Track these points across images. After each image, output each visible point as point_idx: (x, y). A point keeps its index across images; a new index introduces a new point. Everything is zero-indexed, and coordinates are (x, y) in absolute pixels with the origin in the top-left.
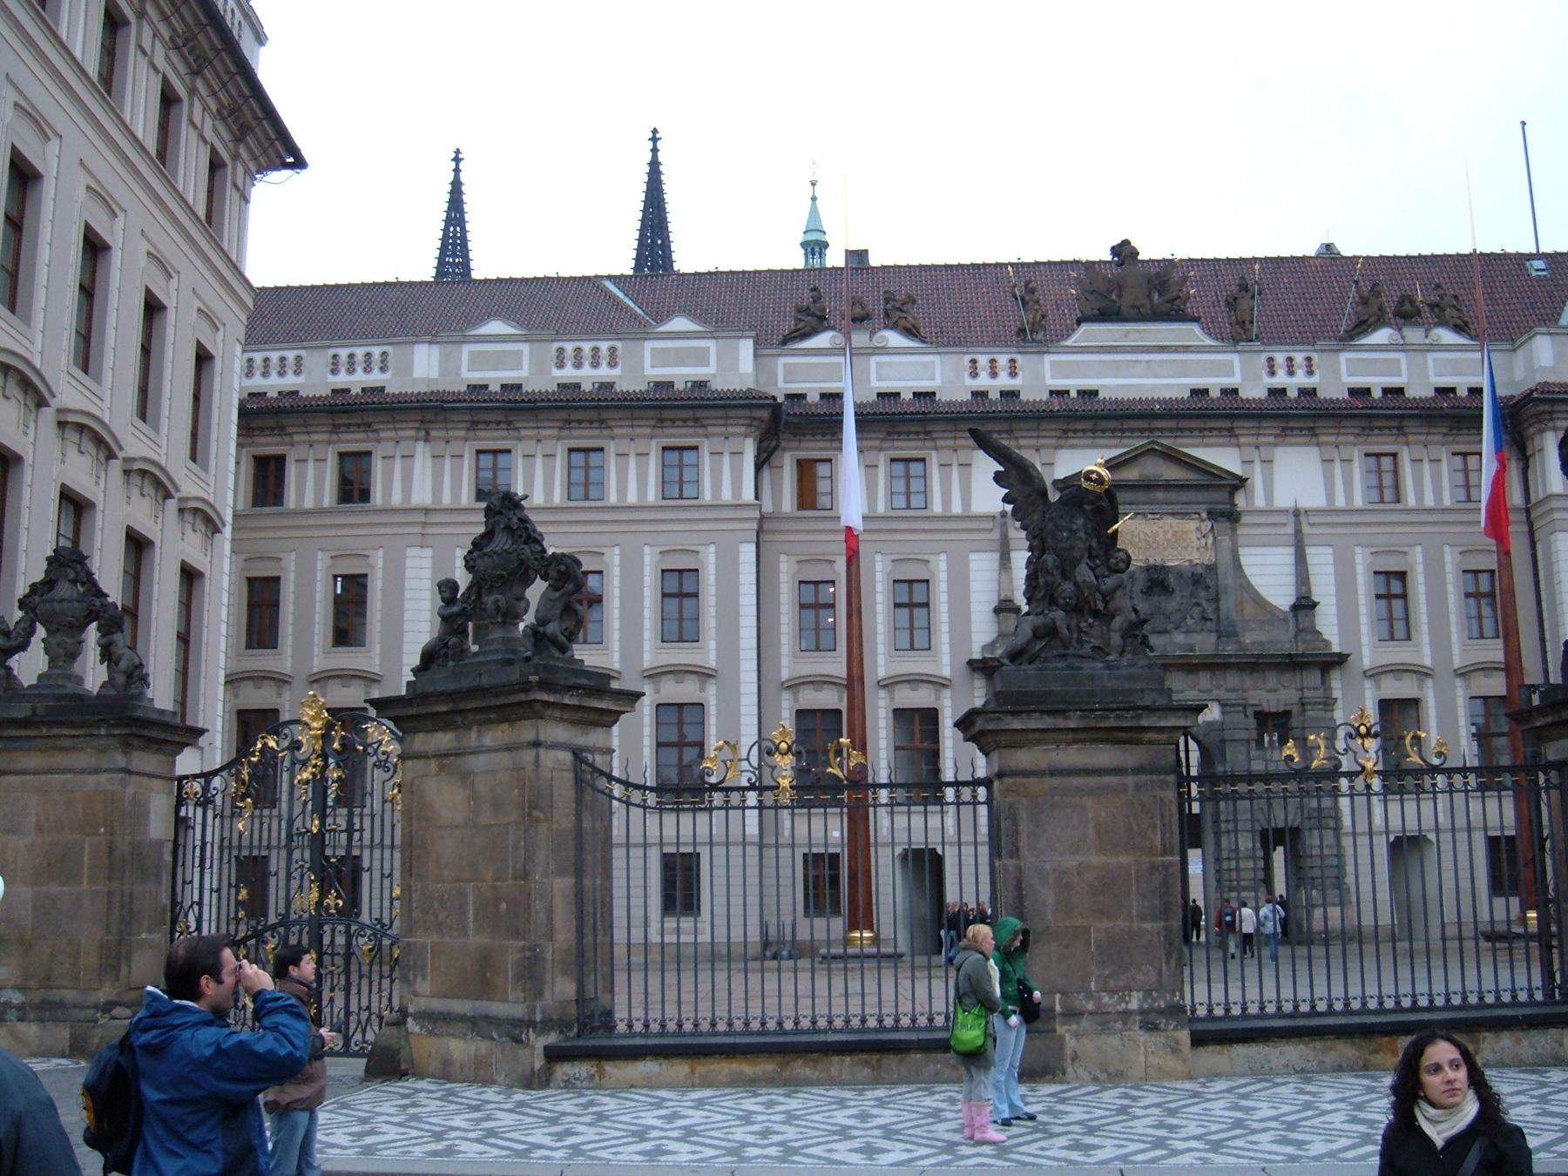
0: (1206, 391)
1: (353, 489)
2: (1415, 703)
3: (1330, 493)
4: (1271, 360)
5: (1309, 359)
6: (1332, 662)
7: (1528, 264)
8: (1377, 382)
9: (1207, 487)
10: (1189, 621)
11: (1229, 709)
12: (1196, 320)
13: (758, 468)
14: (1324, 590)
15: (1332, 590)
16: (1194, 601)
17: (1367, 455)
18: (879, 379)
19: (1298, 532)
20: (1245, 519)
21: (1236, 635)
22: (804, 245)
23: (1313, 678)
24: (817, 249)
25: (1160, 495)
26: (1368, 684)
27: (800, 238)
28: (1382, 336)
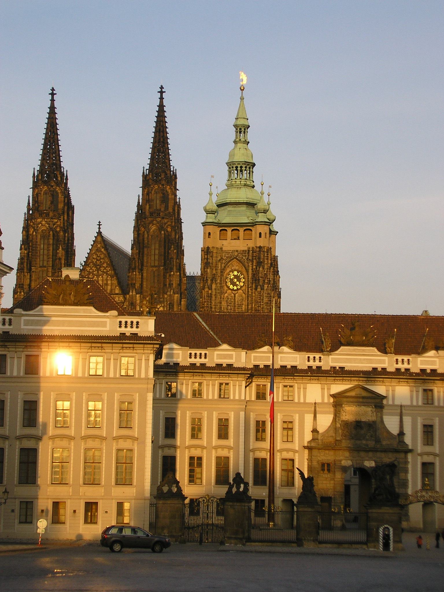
2: (432, 464)
4: (397, 360)
5: (408, 360)
6: (408, 451)
9: (374, 398)
10: (367, 437)
13: (246, 387)
14: (408, 430)
18: (281, 361)
19: (401, 412)
20: (386, 408)
21: (380, 442)
22: (235, 126)
23: (402, 455)
24: (243, 130)
26: (419, 457)
27: (233, 121)
28: (432, 353)
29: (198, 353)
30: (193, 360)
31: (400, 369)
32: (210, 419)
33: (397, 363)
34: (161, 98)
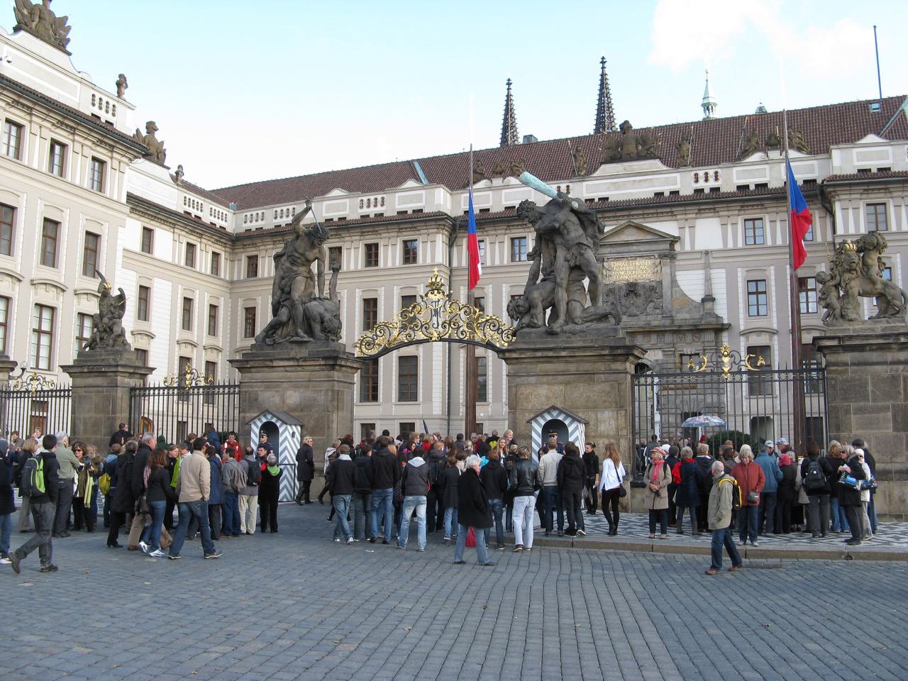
0: (662, 193)
1: (410, 255)
3: (725, 241)
4: (696, 175)
5: (716, 173)
6: (720, 329)
7: (870, 105)
8: (752, 182)
11: (666, 353)
12: (660, 159)
13: (451, 246)
14: (720, 292)
15: (725, 291)
16: (650, 300)
17: (745, 220)
20: (679, 257)
22: (703, 105)
23: (710, 337)
24: (710, 107)
25: (635, 248)
26: (742, 339)
27: (701, 102)
28: (757, 156)
29: (372, 198)
30: (365, 211)
31: (703, 190)
32: (389, 297)
33: (697, 181)
34: (603, 68)
